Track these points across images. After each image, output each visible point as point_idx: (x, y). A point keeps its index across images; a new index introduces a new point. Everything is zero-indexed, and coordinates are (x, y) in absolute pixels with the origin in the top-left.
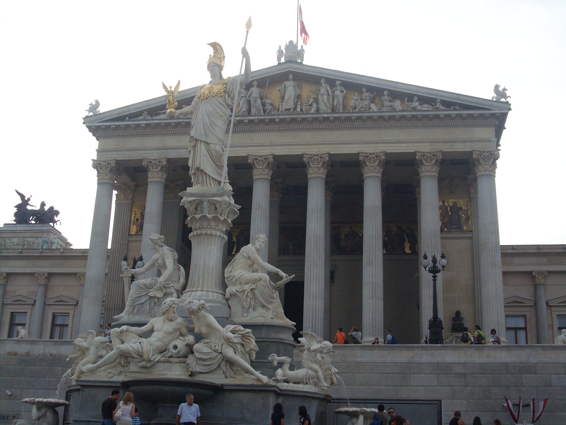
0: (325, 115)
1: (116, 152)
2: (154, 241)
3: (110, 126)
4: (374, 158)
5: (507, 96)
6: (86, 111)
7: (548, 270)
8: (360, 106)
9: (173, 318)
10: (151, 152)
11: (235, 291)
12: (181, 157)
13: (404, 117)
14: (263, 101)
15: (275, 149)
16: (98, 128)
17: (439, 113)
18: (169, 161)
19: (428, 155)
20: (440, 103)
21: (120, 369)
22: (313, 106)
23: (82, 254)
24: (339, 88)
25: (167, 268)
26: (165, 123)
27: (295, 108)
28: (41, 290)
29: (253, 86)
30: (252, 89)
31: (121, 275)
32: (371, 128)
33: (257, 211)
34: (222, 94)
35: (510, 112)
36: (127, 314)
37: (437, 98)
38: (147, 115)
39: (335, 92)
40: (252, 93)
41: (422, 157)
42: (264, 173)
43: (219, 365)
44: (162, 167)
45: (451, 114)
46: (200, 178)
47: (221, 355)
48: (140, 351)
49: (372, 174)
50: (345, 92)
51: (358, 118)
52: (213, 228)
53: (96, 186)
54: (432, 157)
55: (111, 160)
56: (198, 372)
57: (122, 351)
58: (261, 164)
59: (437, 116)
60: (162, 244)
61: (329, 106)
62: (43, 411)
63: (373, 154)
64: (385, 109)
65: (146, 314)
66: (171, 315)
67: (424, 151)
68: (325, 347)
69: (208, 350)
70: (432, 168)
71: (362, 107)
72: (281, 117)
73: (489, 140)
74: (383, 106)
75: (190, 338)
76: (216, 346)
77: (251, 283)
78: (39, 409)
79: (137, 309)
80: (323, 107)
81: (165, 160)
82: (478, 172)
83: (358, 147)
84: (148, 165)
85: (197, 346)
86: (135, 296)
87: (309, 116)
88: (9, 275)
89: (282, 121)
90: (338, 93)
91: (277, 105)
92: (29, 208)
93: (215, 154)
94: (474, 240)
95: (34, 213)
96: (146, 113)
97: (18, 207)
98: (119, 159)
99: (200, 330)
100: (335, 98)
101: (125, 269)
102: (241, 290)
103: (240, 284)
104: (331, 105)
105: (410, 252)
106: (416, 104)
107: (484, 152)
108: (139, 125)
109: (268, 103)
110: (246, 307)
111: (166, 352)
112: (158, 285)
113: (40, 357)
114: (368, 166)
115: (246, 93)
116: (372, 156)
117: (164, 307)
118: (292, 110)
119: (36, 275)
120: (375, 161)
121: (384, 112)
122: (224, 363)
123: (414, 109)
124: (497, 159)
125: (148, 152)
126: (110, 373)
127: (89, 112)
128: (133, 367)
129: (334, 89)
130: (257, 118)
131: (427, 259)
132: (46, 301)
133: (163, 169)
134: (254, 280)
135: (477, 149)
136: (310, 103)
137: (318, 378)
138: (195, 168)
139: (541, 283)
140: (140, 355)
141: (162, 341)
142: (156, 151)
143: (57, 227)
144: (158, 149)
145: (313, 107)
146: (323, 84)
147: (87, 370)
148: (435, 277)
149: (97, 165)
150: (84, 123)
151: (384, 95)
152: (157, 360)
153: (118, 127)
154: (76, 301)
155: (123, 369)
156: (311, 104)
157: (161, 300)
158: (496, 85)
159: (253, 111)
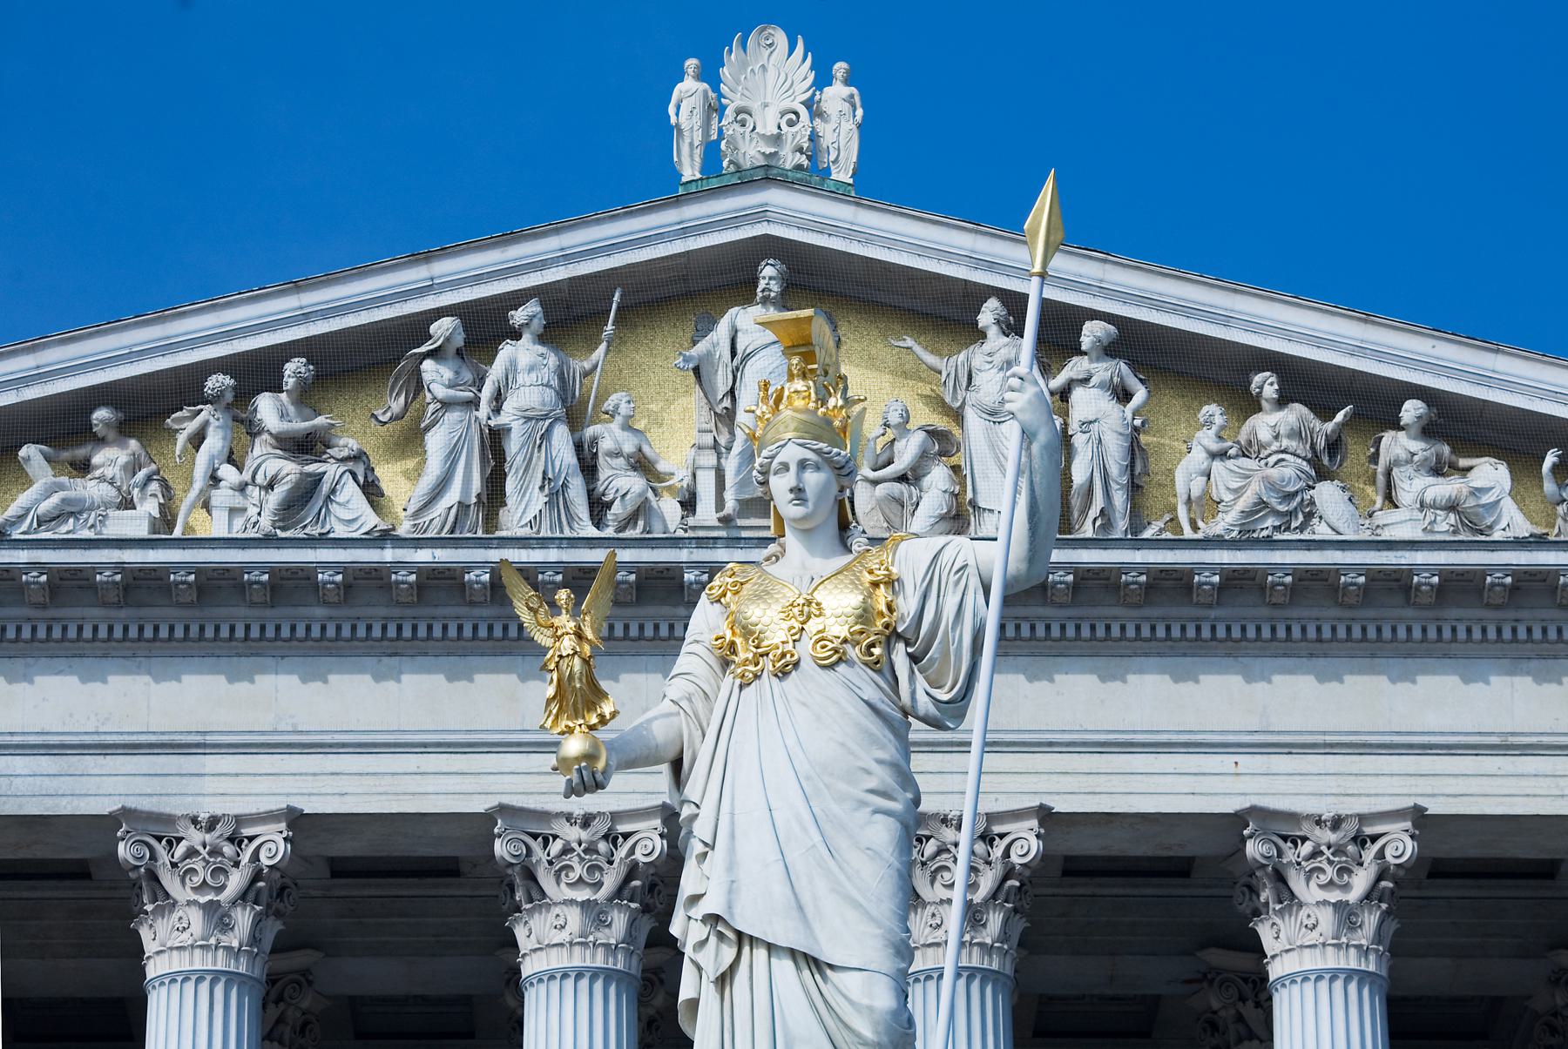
4: (1339, 850)
14: (590, 432)
22: (926, 481)
24: (1104, 370)
29: (516, 335)
30: (506, 351)
34: (877, 651)
39: (1078, 394)
50: (1140, 395)
71: (1261, 504)
91: (681, 478)
156: (914, 469)
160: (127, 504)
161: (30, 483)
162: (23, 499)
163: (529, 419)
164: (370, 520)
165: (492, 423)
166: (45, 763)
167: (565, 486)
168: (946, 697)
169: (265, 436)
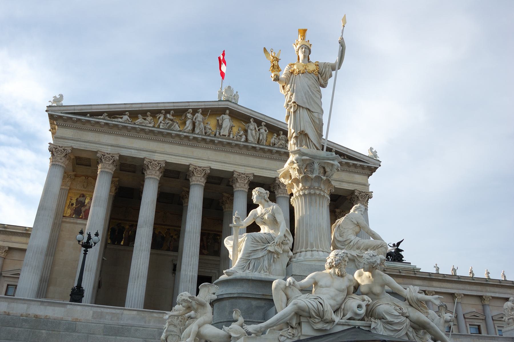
0: (254, 145)
1: (72, 141)
3: (71, 118)
6: (50, 101)
8: (279, 143)
9: (344, 273)
10: (104, 147)
12: (131, 156)
15: (211, 164)
18: (121, 157)
23: (3, 229)
24: (264, 128)
26: (122, 126)
27: (229, 136)
29: (198, 112)
30: (197, 114)
33: (194, 210)
36: (240, 269)
37: (333, 148)
38: (107, 116)
39: (261, 130)
42: (201, 181)
44: (114, 161)
46: (304, 141)
50: (267, 131)
51: (277, 152)
58: (199, 173)
61: (256, 139)
72: (220, 140)
73: (365, 185)
79: (253, 264)
83: (275, 174)
84: (101, 157)
86: (251, 250)
87: (241, 143)
89: (220, 143)
90: (262, 131)
93: (318, 122)
100: (261, 134)
104: (258, 139)
107: (362, 192)
108: (98, 122)
109: (208, 128)
113: (22, 317)
115: (192, 116)
118: (227, 136)
122: (411, 329)
124: (371, 198)
125: (103, 146)
126: (281, 335)
127: (53, 103)
130: (200, 136)
133: (114, 163)
134: (375, 246)
135: (358, 189)
136: (241, 134)
140: (321, 315)
141: (335, 300)
142: (110, 147)
145: (242, 138)
146: (252, 122)
147: (254, 330)
149: (53, 150)
150: (47, 111)
158: (371, 147)
159: (197, 131)
162: (138, 120)
163: (199, 121)
169: (167, 119)
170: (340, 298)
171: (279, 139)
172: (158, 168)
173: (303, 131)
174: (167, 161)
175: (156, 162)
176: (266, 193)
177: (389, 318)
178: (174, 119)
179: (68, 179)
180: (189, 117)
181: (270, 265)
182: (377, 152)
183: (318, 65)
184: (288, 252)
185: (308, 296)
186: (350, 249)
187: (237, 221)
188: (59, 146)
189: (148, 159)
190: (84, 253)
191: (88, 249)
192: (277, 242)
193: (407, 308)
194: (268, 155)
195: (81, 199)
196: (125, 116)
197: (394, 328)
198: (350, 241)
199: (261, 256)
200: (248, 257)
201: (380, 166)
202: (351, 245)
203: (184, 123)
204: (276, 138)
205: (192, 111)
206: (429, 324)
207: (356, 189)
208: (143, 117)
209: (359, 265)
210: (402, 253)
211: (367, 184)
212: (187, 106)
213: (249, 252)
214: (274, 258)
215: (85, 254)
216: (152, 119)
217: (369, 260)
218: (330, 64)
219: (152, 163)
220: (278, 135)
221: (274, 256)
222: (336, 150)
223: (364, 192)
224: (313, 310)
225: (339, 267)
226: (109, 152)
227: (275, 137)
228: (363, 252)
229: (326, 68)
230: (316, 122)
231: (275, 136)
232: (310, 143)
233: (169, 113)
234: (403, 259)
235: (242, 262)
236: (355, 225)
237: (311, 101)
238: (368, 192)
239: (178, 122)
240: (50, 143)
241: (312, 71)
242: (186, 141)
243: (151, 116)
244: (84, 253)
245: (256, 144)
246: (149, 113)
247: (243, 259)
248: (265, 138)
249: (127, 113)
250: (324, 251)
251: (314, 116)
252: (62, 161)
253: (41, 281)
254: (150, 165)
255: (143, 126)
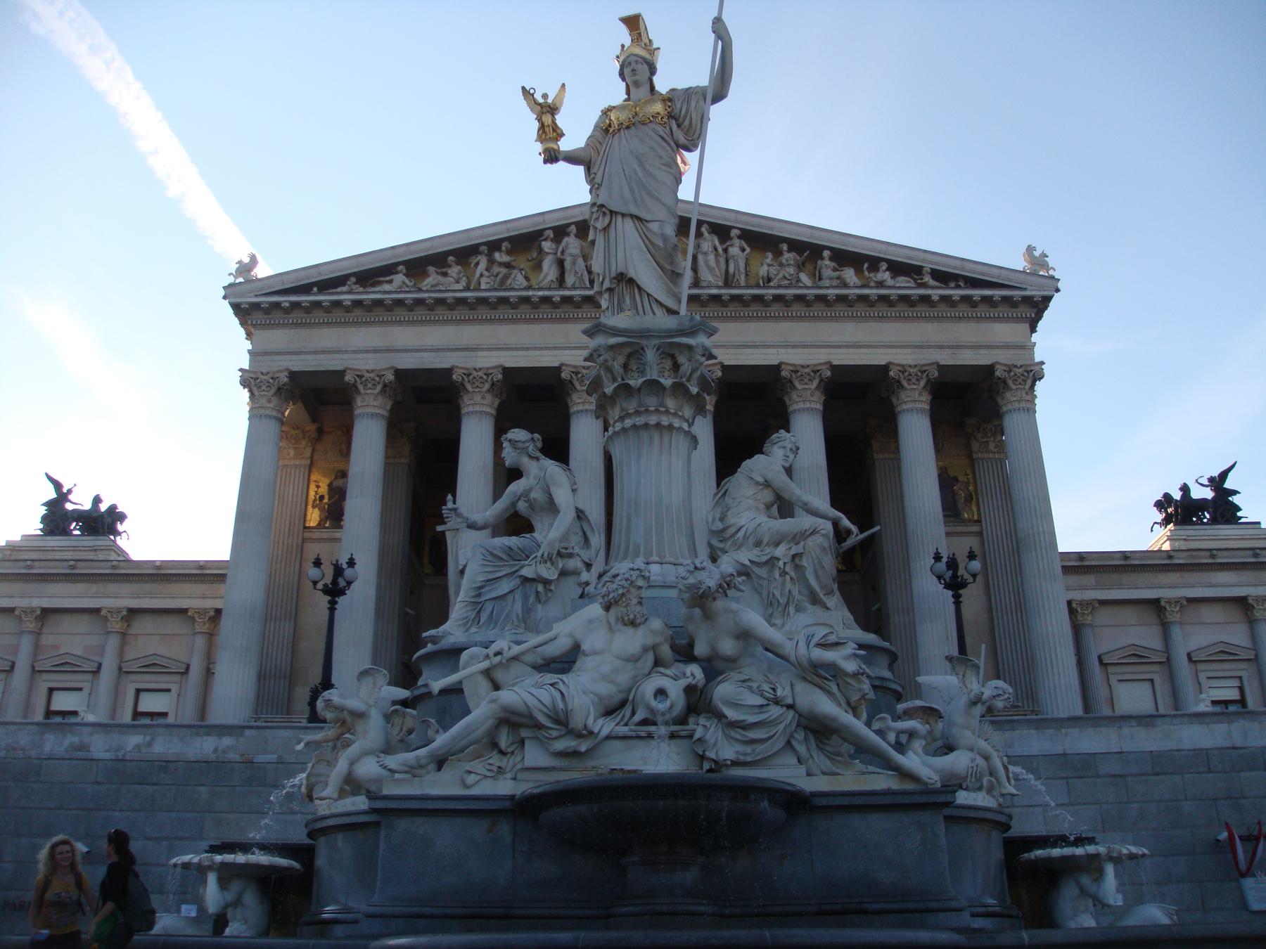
0: (714, 291)
2: (520, 445)
4: (809, 374)
5: (1050, 266)
6: (230, 274)
7: (1100, 598)
8: (781, 276)
9: (638, 616)
11: (747, 563)
13: (863, 299)
16: (256, 306)
17: (929, 292)
18: (399, 373)
19: (912, 370)
20: (929, 276)
21: (495, 760)
24: (737, 242)
25: (559, 512)
26: (393, 300)
28: (113, 642)
29: (568, 235)
30: (566, 239)
31: (439, 528)
32: (801, 318)
34: (665, 120)
35: (1056, 295)
37: (924, 265)
38: (355, 284)
39: (730, 249)
40: (567, 246)
41: (901, 374)
43: (789, 743)
45: (950, 296)
47: (791, 713)
48: (561, 706)
49: (808, 405)
50: (748, 250)
51: (778, 299)
52: (671, 413)
53: (245, 424)
54: (920, 374)
55: (279, 371)
56: (729, 763)
57: (505, 709)
59: (925, 299)
60: (539, 454)
61: (718, 274)
62: (236, 886)
63: (808, 366)
64: (827, 283)
65: (516, 623)
66: (635, 610)
67: (905, 362)
68: (998, 695)
69: (760, 701)
70: (920, 395)
73: (1022, 346)
74: (820, 279)
75: (695, 673)
76: (774, 689)
77: (789, 542)
78: (223, 883)
79: (488, 612)
80: (706, 276)
81: (392, 371)
82: (1005, 405)
85: (724, 690)
88: (47, 612)
90: (734, 251)
92: (69, 506)
93: (661, 245)
94: (985, 536)
95: (80, 516)
96: (353, 279)
97: (50, 504)
98: (295, 369)
99: (714, 649)
101: (451, 510)
102: (764, 559)
103: (758, 544)
104: (723, 274)
105: (844, 568)
106: (884, 276)
108: (338, 304)
110: (783, 601)
111: (627, 711)
112: (544, 549)
114: (797, 389)
115: (554, 246)
116: (807, 370)
117: (614, 586)
119: (102, 613)
120: (812, 381)
121: (827, 288)
122: (800, 735)
123: (881, 284)
126: (470, 772)
127: (236, 277)
128: (534, 755)
129: (728, 244)
130: (578, 292)
131: (941, 561)
132: (123, 665)
134: (796, 535)
137: (992, 773)
138: (613, 275)
139: (1088, 622)
140: (561, 720)
141: (612, 682)
142: (371, 355)
143: (121, 542)
144: (376, 351)
146: (706, 234)
147: (400, 764)
148: (957, 597)
149: (248, 380)
150: (225, 298)
151: (822, 259)
152: (605, 732)
153: (295, 305)
154: (184, 666)
155: (505, 760)
157: (552, 587)
159: (570, 280)
160: (458, 282)
161: (429, 276)
164: (525, 283)
165: (562, 257)
166: (433, 354)
167: (582, 275)
168: (690, 139)
170: (624, 678)
171: (781, 265)
172: (487, 386)
173: (622, 274)
174: (507, 366)
175: (482, 371)
176: (533, 439)
177: (731, 714)
178: (512, 261)
179: (304, 443)
180: (546, 250)
181: (528, 611)
182: (1047, 257)
183: (670, 100)
184: (579, 574)
185: (542, 679)
186: (736, 548)
187: (451, 517)
188: (262, 373)
189: (464, 368)
190: (328, 608)
191: (337, 599)
192: (543, 555)
193: (792, 685)
194: (755, 309)
195: (339, 483)
196: (397, 275)
197: (745, 736)
198: (735, 530)
199: (506, 591)
200: (476, 596)
201: (1058, 290)
202: (738, 539)
203: (538, 266)
204: (770, 263)
205: (554, 233)
206: (835, 719)
207: (996, 362)
208: (439, 271)
209: (761, 585)
210: (1235, 499)
211: (1029, 344)
212: (541, 223)
213: (477, 585)
214: (537, 592)
215: (332, 609)
216: (462, 271)
217: (685, 582)
218: (700, 91)
219: (471, 377)
220: (778, 254)
221: (537, 588)
222: (931, 269)
223: (1021, 366)
224: (540, 711)
225: (624, 605)
226: (369, 367)
227: (768, 261)
228: (766, 553)
229: (688, 103)
230: (658, 246)
231: (769, 259)
232: (644, 300)
233: (499, 250)
234: (1239, 514)
235: (465, 610)
236: (761, 485)
237: (643, 193)
238: (1030, 365)
239: (522, 267)
240: (241, 370)
241: (649, 118)
242: (545, 308)
243: (458, 263)
244: (328, 608)
245: (718, 287)
246: (451, 258)
247: (465, 603)
248: (742, 270)
249: (401, 268)
250: (664, 561)
251: (651, 231)
252: (271, 405)
253: (262, 677)
254: (469, 382)
255: (440, 291)
